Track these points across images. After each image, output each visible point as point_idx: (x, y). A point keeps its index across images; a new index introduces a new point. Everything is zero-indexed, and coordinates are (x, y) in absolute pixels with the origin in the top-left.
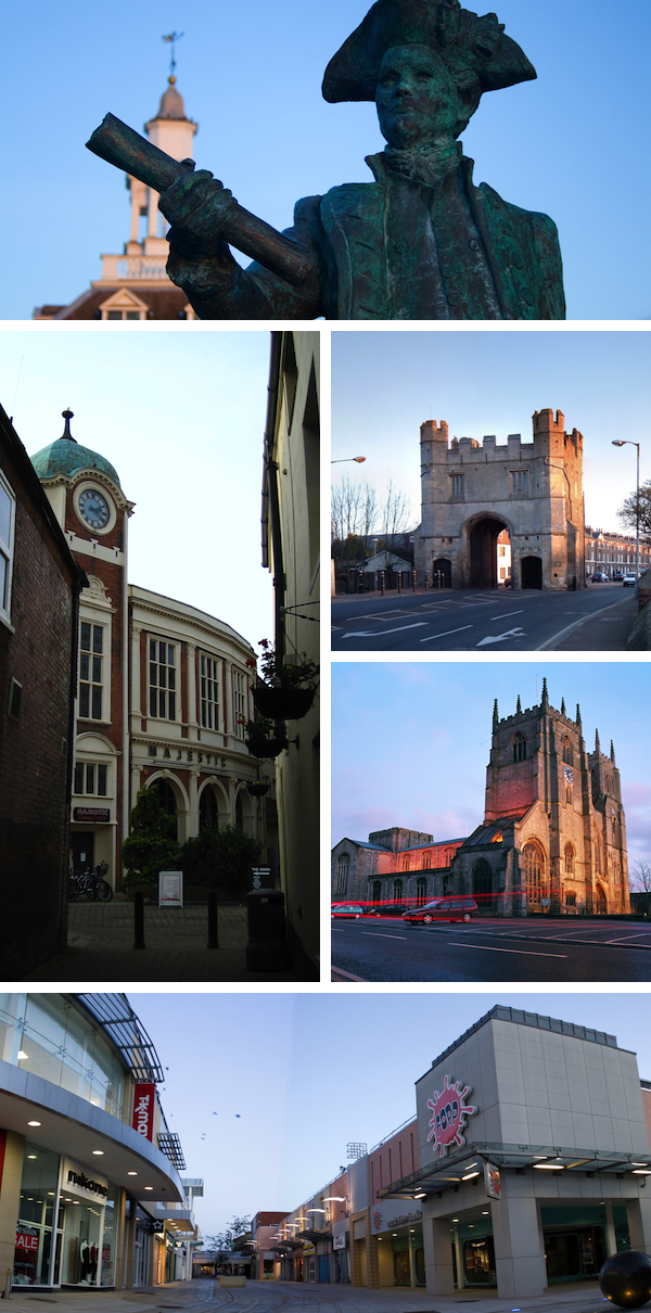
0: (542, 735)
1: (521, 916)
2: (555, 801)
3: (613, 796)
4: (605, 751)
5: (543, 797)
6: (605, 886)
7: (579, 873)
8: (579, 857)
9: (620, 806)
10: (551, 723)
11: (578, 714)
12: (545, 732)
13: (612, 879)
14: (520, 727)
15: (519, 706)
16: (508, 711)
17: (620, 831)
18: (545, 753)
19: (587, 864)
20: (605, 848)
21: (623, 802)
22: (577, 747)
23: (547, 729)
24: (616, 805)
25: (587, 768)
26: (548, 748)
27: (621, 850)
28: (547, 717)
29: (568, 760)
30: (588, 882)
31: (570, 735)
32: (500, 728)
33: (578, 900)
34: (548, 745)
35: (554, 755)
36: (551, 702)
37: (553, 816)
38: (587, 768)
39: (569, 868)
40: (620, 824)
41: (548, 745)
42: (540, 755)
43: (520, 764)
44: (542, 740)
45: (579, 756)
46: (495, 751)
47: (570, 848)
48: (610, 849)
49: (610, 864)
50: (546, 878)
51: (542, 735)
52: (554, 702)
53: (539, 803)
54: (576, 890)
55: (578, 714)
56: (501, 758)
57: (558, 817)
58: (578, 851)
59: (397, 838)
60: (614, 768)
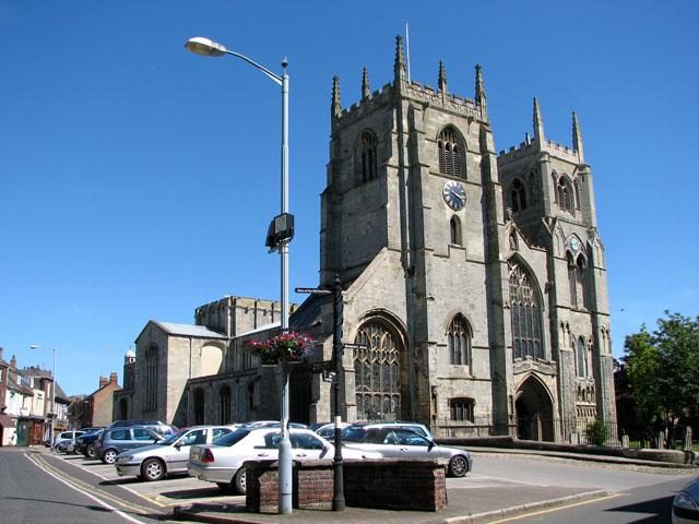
3: (579, 217)
7: (481, 363)
8: (480, 336)
10: (411, 111)
13: (569, 368)
14: (368, 123)
16: (349, 99)
18: (401, 166)
19: (495, 348)
20: (553, 315)
23: (405, 122)
25: (495, 178)
27: (594, 315)
28: (405, 104)
31: (460, 124)
32: (339, 126)
33: (478, 411)
34: (406, 150)
35: (415, 167)
37: (414, 271)
38: (495, 178)
39: (456, 358)
42: (392, 174)
43: (369, 184)
44: (395, 145)
45: (478, 159)
46: (335, 168)
47: (460, 324)
48: (563, 315)
49: (564, 342)
51: (394, 137)
53: (385, 253)
56: (344, 177)
59: (233, 315)
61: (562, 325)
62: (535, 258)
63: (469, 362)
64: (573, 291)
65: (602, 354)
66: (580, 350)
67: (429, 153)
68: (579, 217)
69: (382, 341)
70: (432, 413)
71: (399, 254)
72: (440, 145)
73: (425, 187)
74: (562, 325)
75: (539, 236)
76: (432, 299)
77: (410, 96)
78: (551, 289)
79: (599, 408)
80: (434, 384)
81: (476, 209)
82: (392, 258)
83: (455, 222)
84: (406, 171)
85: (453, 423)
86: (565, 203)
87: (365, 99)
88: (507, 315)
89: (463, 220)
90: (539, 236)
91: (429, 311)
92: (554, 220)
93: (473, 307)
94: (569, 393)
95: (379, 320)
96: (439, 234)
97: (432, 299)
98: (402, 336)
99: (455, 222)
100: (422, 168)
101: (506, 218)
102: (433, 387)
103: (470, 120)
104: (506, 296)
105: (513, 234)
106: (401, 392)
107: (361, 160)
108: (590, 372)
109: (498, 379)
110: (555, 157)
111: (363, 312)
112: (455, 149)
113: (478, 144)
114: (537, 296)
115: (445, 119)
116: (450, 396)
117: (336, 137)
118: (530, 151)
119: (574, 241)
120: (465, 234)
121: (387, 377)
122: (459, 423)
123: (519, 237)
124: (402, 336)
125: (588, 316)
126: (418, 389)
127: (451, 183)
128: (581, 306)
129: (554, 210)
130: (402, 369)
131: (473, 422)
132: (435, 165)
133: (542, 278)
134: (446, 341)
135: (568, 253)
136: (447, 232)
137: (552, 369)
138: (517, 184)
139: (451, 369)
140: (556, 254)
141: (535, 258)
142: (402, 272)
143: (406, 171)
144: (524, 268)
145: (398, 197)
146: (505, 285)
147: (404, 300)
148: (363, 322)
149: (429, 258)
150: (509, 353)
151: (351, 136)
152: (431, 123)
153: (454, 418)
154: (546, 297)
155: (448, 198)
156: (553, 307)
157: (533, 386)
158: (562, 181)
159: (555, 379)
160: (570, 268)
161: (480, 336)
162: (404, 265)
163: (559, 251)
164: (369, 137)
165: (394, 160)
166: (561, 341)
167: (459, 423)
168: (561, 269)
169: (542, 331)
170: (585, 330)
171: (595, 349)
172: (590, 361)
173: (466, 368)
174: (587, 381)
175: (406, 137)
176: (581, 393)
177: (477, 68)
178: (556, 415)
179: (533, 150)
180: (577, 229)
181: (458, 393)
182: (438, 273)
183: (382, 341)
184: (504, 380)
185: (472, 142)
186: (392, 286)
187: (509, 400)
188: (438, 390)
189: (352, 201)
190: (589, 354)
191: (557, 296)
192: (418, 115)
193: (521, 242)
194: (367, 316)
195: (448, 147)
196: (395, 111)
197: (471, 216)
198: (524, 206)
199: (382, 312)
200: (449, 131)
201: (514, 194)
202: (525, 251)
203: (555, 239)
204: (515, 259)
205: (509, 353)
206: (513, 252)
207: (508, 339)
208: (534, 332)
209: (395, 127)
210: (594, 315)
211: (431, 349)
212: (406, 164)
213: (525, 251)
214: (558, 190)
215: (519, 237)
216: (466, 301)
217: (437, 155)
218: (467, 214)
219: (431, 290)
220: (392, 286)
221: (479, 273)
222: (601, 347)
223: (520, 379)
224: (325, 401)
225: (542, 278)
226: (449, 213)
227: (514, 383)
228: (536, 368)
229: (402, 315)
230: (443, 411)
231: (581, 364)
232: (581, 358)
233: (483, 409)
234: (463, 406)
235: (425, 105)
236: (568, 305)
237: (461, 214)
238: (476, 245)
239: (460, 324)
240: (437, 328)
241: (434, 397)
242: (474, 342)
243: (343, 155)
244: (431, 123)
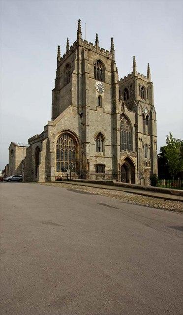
0: (76, 62)
1: (50, 181)
2: (84, 106)
3: (148, 102)
4: (141, 70)
5: (76, 103)
6: (134, 160)
7: (108, 151)
8: (108, 141)
9: (152, 107)
11: (112, 45)
12: (78, 60)
13: (141, 155)
15: (68, 46)
17: (151, 124)
18: (78, 74)
19: (114, 146)
20: (136, 135)
21: (155, 104)
22: (108, 68)
23: (80, 56)
24: (149, 107)
26: (80, 70)
27: (151, 136)
28: (80, 48)
29: (100, 76)
30: (114, 158)
31: (103, 60)
32: (60, 62)
33: (106, 169)
34: (80, 67)
35: (84, 74)
36: (83, 37)
37: (82, 115)
39: (98, 149)
40: (151, 119)
41: (80, 67)
45: (110, 74)
46: (57, 80)
48: (140, 136)
49: (140, 144)
50: (78, 156)
51: (76, 62)
52: (88, 37)
54: (105, 163)
55: (112, 45)
56: (61, 84)
57: (85, 116)
58: (107, 137)
60: (150, 84)
61: (140, 139)
62: (131, 115)
63: (103, 151)
64: (144, 128)
65: (153, 150)
66: (146, 149)
67: (89, 68)
68: (148, 102)
69: (69, 142)
70: (87, 169)
72: (95, 67)
73: (87, 82)
74: (140, 139)
75: (132, 107)
76: (88, 125)
77: (83, 45)
78: (136, 126)
79: (152, 169)
81: (108, 93)
82: (73, 111)
83: (100, 97)
84: (80, 76)
85: (97, 174)
86: (143, 97)
87: (67, 50)
88: (118, 133)
89: (103, 97)
90: (132, 107)
91: (87, 130)
92: (139, 101)
93: (105, 130)
94: (141, 163)
96: (93, 102)
97: (88, 125)
99: (100, 97)
100: (86, 74)
101: (120, 99)
103: (108, 58)
104: (118, 127)
105: (123, 105)
107: (66, 76)
108: (149, 156)
109: (114, 158)
110: (140, 79)
111: (60, 130)
112: (101, 70)
113: (110, 69)
114: (131, 128)
115: (97, 57)
116: (95, 163)
117: (58, 69)
118: (131, 77)
119: (145, 110)
120: (104, 103)
122: (99, 174)
123: (125, 106)
125: (149, 137)
126: (82, 161)
127: (98, 83)
128: (147, 133)
129: (139, 98)
131: (104, 173)
132: (92, 75)
133: (133, 122)
134: (95, 143)
135: (143, 115)
136: (97, 101)
137: (135, 155)
138: (126, 90)
139: (97, 154)
140: (139, 113)
141: (131, 115)
143: (80, 76)
144: (127, 118)
145: (77, 86)
146: (119, 122)
149: (88, 110)
150: (119, 148)
151: (63, 68)
152: (91, 58)
153: (97, 171)
154: (134, 129)
155: (97, 88)
156: (137, 133)
157: (128, 159)
158: (142, 88)
159: (136, 158)
160: (143, 119)
161: (108, 141)
162: (78, 112)
163: (140, 113)
164: (68, 66)
165: (75, 71)
166: (139, 145)
167: (99, 174)
168: (140, 119)
169: (132, 141)
170: (148, 142)
171: (151, 148)
172: (149, 152)
173: (102, 153)
174: (148, 160)
175: (80, 62)
176: (145, 164)
177: (112, 39)
178: (136, 171)
179: (131, 77)
180: (147, 106)
181: (99, 162)
182: (91, 115)
183: (69, 142)
184: (117, 158)
185: (108, 68)
187: (118, 165)
188: (90, 161)
189: (62, 92)
190: (149, 150)
191: (138, 128)
192: (86, 53)
193: (126, 108)
195: (98, 69)
196: (76, 50)
197: (106, 97)
198: (128, 98)
199: (68, 131)
200: (99, 62)
201: (125, 93)
202: (127, 112)
203: (138, 108)
204: (123, 115)
205: (119, 148)
206: (122, 112)
207: (119, 143)
208: (129, 141)
209: (76, 58)
210: (151, 136)
211: (87, 145)
212: (80, 73)
213: (127, 112)
214: (141, 91)
215: (125, 106)
216: (103, 128)
217: (93, 71)
218: (105, 95)
219: (88, 122)
221: (108, 118)
222: (153, 148)
223: (123, 157)
225: (133, 122)
226: (97, 94)
227: (121, 160)
228: (129, 154)
229: (77, 132)
230: (92, 168)
231: (146, 153)
232: (146, 151)
233: (109, 167)
234: (100, 167)
235: (89, 50)
236: (142, 132)
237: (102, 95)
238: (108, 107)
239: (100, 137)
240: (90, 137)
241: (88, 163)
242: (105, 143)
243: (60, 76)
244: (91, 58)
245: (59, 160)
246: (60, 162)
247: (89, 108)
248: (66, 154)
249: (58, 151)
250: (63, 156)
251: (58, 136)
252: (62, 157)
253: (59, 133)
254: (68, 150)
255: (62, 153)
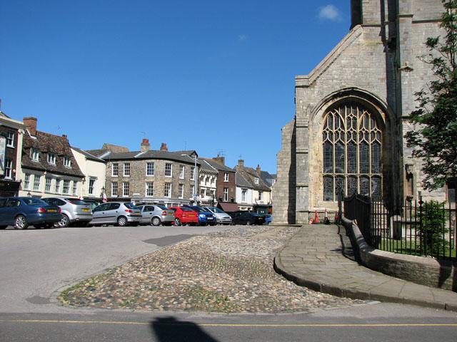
70: (407, 192)
71: (379, 29)
80: (409, 162)
82: (367, 37)
95: (349, 100)
97: (408, 69)
98: (383, 115)
102: (407, 166)
106: (384, 172)
111: (328, 92)
121: (364, 157)
124: (383, 115)
130: (384, 148)
142: (382, 47)
147: (384, 75)
148: (330, 103)
183: (359, 121)
186: (366, 63)
194: (335, 97)
199: (353, 91)
220: (366, 63)
224: (283, 183)
229: (381, 93)
245: (331, 171)
246: (334, 174)
247: (410, 20)
248: (352, 155)
249: (327, 146)
250: (343, 159)
251: (325, 108)
252: (340, 162)
253: (326, 101)
254: (358, 143)
255: (339, 151)
